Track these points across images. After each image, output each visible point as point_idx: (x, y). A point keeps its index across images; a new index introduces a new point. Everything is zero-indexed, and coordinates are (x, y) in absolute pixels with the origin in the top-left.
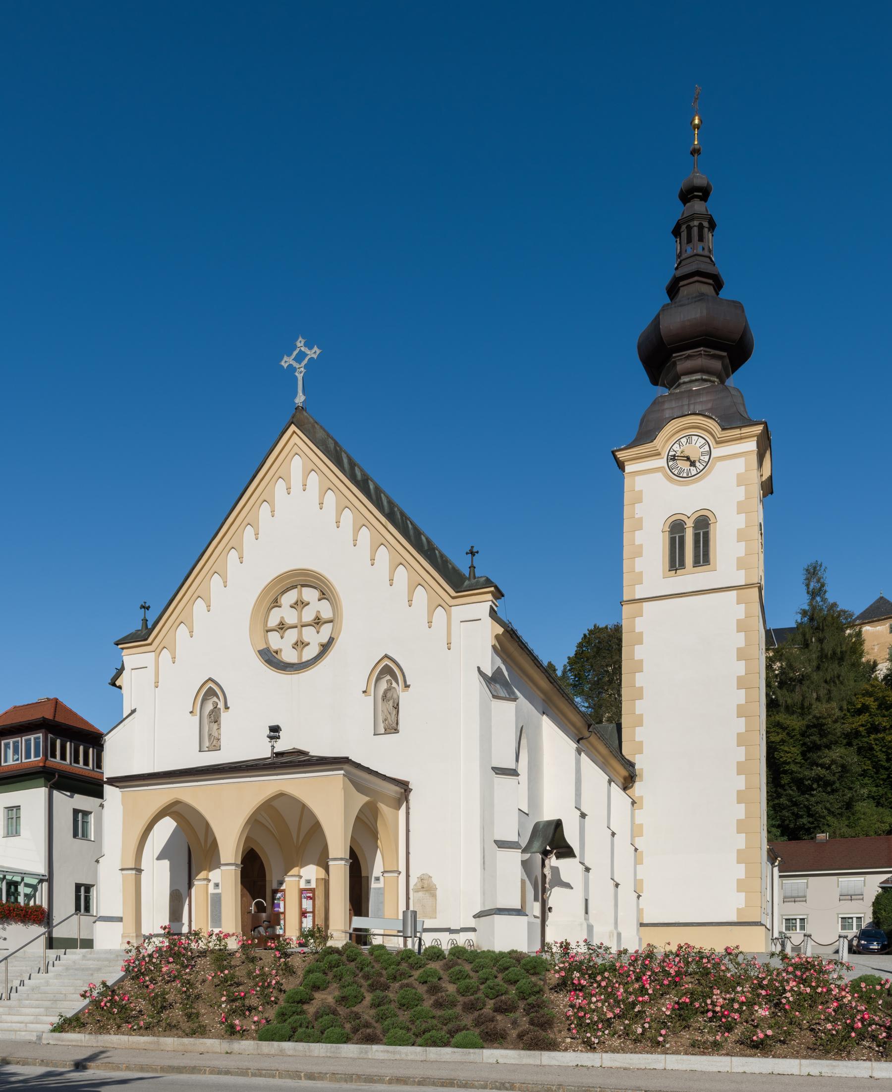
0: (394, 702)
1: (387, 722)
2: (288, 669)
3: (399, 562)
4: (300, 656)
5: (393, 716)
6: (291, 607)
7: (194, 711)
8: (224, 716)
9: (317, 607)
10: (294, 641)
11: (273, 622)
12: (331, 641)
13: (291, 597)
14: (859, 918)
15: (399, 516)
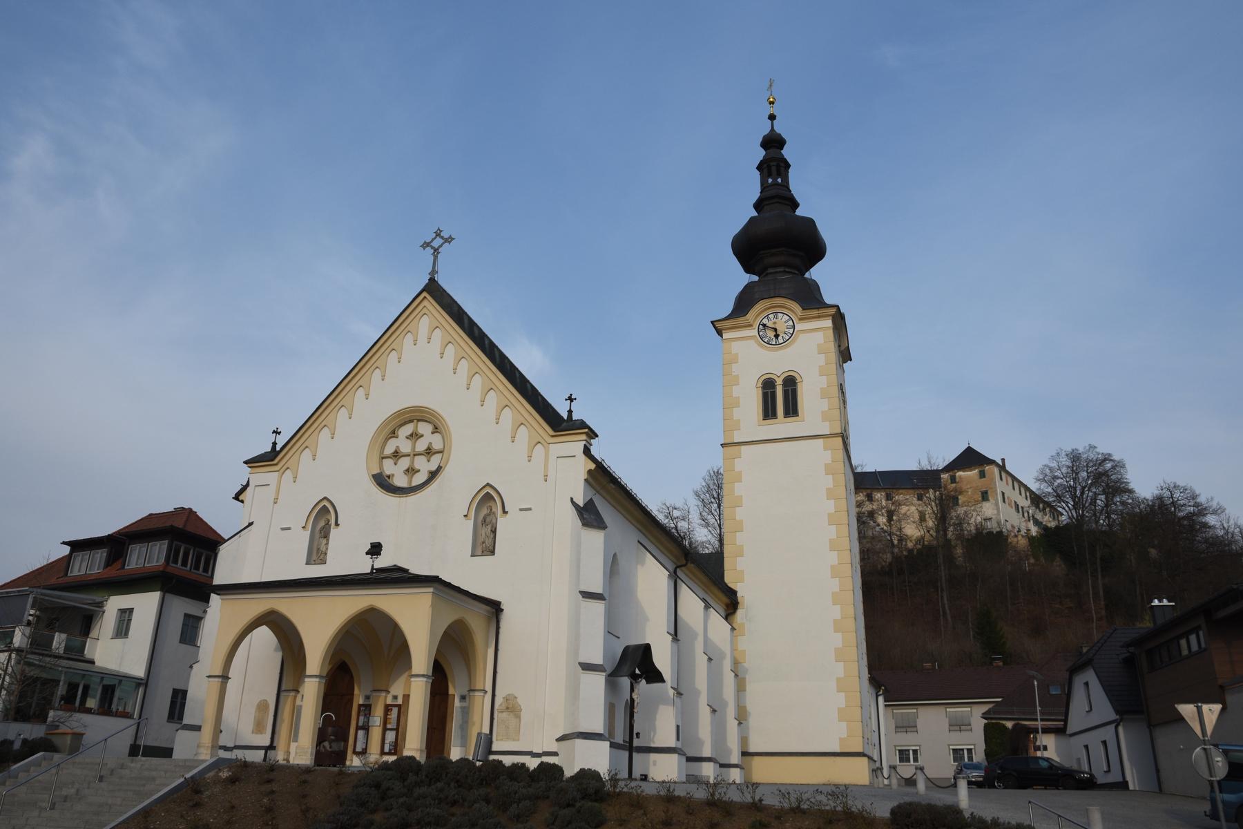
0: (492, 527)
1: (484, 545)
2: (397, 492)
3: (505, 404)
4: (410, 481)
5: (490, 540)
6: (407, 438)
7: (307, 527)
8: (334, 532)
9: (429, 438)
10: (406, 468)
11: (389, 450)
12: (439, 469)
13: (408, 429)
14: (970, 751)
15: (509, 367)
